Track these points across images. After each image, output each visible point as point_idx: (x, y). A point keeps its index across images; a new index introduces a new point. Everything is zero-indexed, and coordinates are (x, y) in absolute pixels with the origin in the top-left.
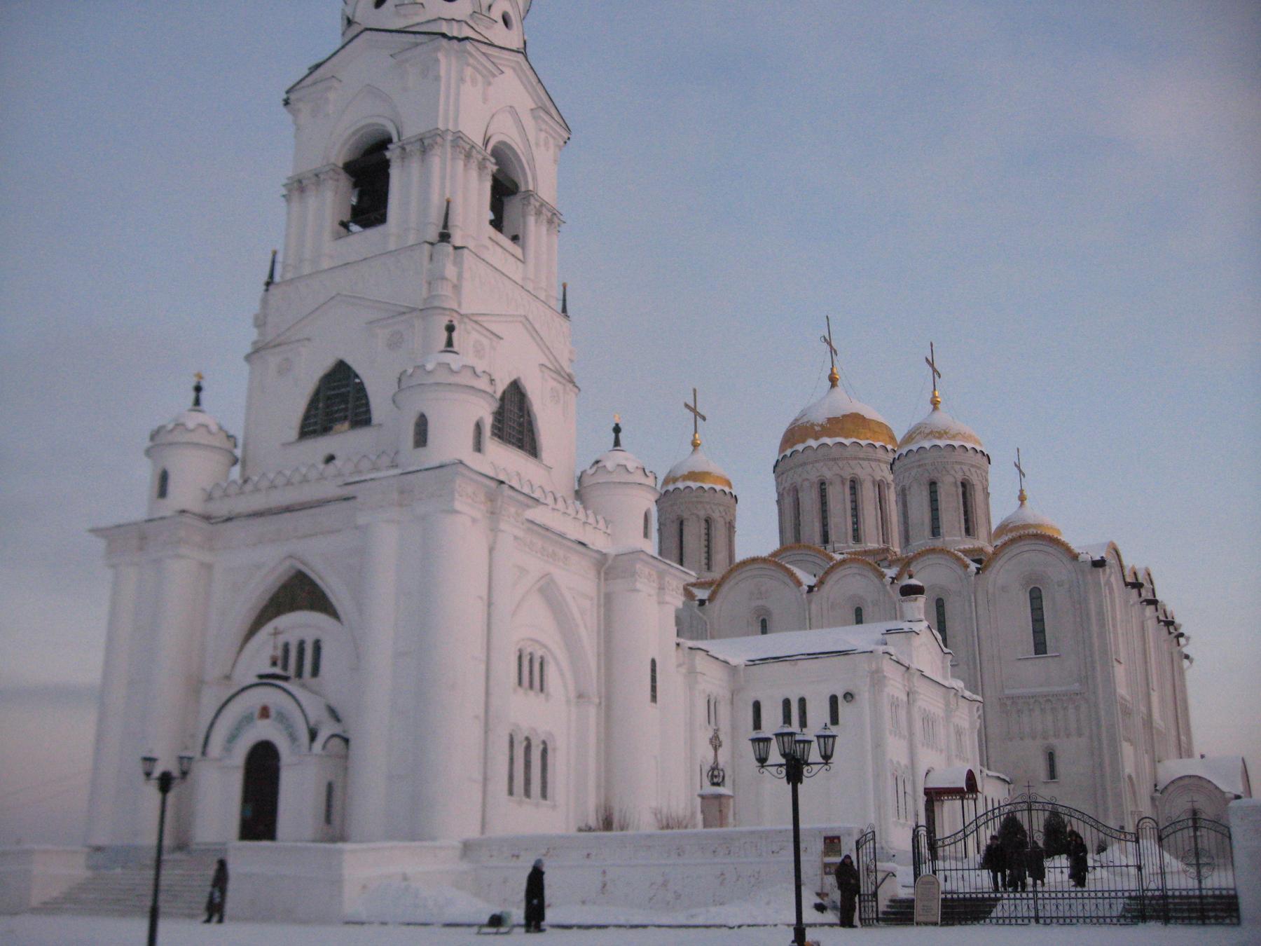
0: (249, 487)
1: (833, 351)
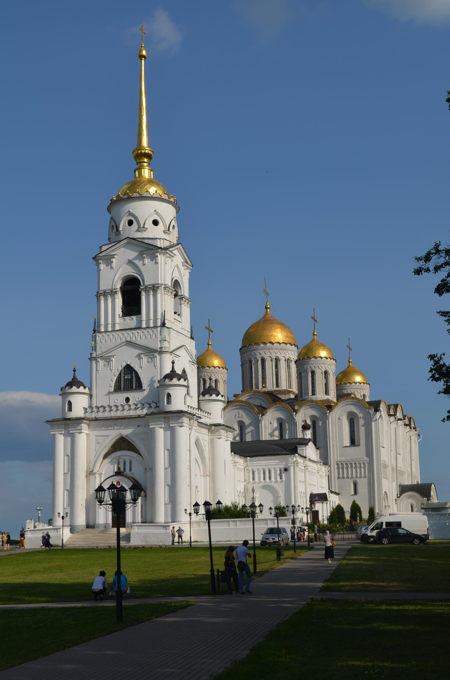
0: (101, 409)
1: (267, 294)
